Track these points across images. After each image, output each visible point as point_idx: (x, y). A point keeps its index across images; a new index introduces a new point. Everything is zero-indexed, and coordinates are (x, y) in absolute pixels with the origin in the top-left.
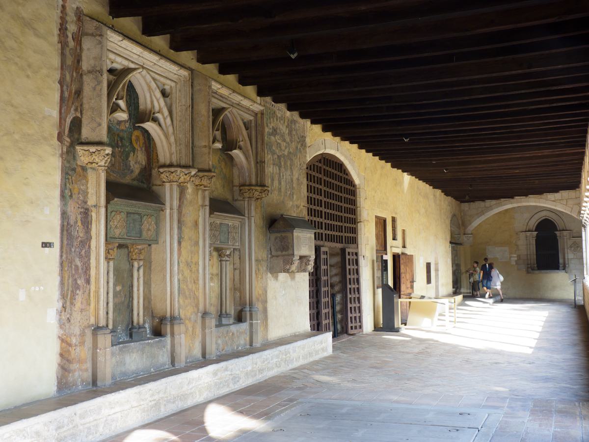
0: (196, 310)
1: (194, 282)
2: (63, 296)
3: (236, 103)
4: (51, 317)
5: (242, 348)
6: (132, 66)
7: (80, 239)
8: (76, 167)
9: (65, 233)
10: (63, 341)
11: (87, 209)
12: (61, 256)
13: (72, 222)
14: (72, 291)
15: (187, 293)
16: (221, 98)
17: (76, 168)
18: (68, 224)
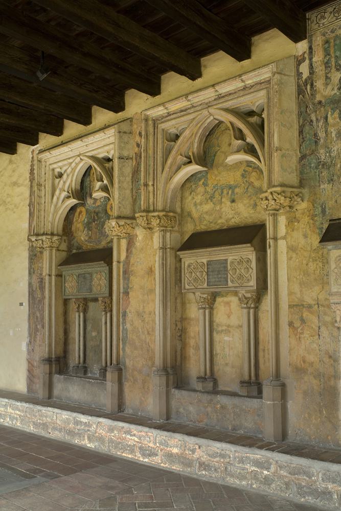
0: (150, 363)
1: (148, 333)
2: (30, 335)
3: (215, 100)
4: (24, 347)
5: (245, 432)
6: (71, 161)
7: (38, 299)
8: (36, 253)
9: (31, 296)
10: (29, 362)
11: (42, 279)
12: (29, 311)
13: (34, 289)
14: (35, 333)
15: (137, 344)
16: (185, 113)
17: (36, 254)
18: (32, 290)
